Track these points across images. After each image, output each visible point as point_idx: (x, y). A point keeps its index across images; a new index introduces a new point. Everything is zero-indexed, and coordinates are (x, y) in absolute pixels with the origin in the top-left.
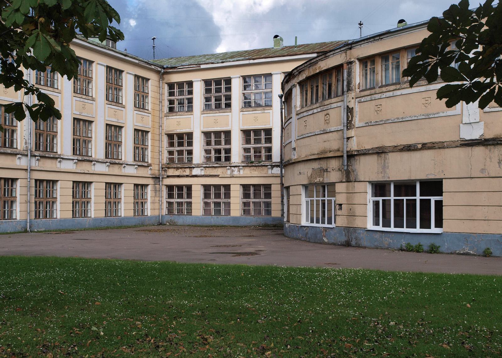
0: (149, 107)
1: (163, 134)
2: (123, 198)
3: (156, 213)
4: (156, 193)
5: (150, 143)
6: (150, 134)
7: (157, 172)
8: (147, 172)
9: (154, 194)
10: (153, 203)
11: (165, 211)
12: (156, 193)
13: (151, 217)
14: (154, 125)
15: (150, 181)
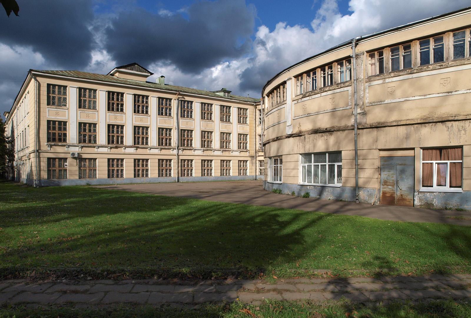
0: (248, 122)
1: (257, 135)
2: (232, 167)
3: (254, 174)
4: (252, 164)
5: (248, 140)
6: (248, 136)
7: (253, 154)
8: (247, 154)
9: (251, 165)
10: (251, 169)
11: (258, 173)
12: (252, 164)
13: (250, 176)
14: (251, 131)
15: (249, 159)
